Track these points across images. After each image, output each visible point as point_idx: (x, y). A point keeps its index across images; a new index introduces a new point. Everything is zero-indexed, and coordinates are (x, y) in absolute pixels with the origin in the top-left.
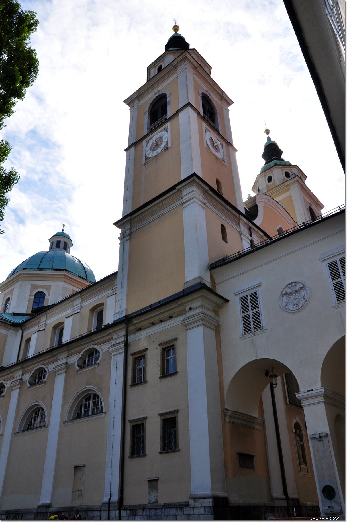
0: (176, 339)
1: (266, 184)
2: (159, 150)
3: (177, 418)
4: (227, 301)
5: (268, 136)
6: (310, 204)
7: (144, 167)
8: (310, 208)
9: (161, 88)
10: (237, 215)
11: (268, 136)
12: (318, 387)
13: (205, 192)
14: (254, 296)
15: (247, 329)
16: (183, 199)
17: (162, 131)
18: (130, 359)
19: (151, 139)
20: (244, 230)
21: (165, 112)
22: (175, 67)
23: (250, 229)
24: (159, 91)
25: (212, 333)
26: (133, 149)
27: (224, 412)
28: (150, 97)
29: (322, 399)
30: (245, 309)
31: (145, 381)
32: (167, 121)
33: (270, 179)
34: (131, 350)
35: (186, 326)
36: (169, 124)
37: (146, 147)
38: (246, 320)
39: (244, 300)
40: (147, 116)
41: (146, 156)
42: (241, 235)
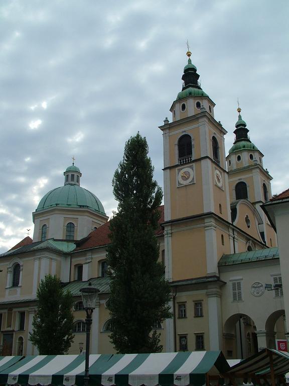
0: (203, 300)
3: (205, 337)
4: (226, 283)
6: (264, 181)
8: (264, 185)
9: (187, 129)
10: (228, 225)
12: (264, 330)
13: (216, 219)
14: (239, 284)
15: (235, 299)
16: (206, 224)
17: (189, 167)
18: (177, 305)
19: (181, 169)
20: (231, 231)
21: (190, 153)
22: (198, 118)
23: (233, 230)
24: (185, 131)
25: (219, 299)
26: (168, 170)
27: (223, 333)
28: (178, 133)
29: (265, 335)
30: (234, 289)
31: (185, 317)
32: (191, 162)
33: (239, 158)
34: (177, 301)
35: (208, 295)
36: (194, 164)
38: (234, 295)
39: (234, 285)
42: (229, 236)
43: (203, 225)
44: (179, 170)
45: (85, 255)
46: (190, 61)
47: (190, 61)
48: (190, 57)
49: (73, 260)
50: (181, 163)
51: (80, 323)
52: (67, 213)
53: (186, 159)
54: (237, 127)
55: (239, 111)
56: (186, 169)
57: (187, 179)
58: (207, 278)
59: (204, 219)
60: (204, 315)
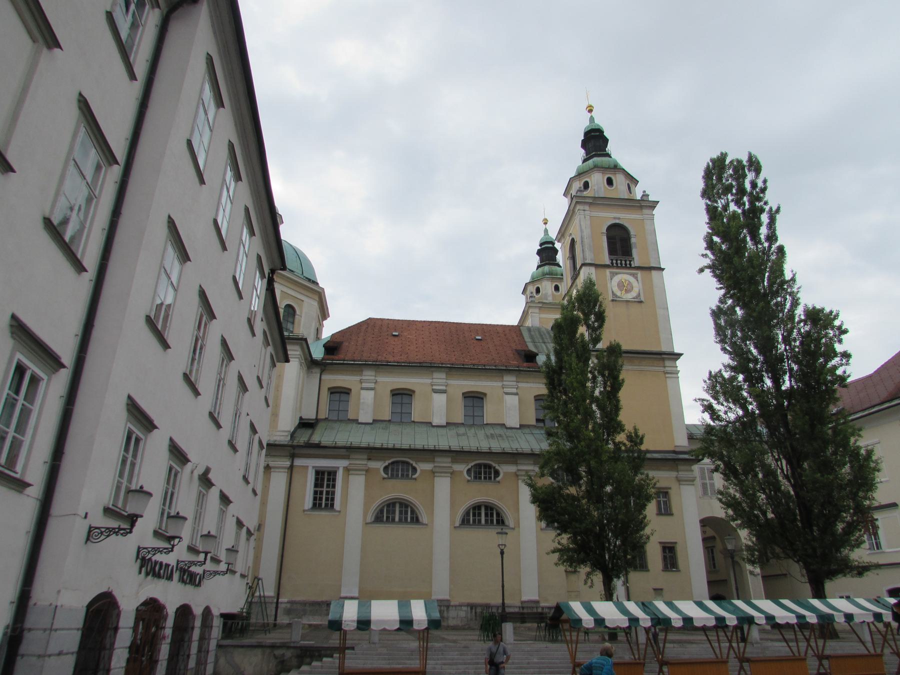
1: (552, 291)
2: (630, 296)
3: (679, 550)
5: (546, 228)
7: (611, 303)
11: (546, 228)
17: (631, 275)
19: (617, 274)
24: (619, 219)
28: (611, 216)
36: (639, 274)
37: (611, 279)
40: (605, 239)
41: (613, 292)
43: (662, 369)
44: (613, 275)
45: (360, 373)
46: (592, 119)
47: (592, 119)
48: (593, 114)
49: (323, 377)
50: (612, 263)
51: (394, 504)
52: (289, 285)
53: (621, 261)
54: (541, 245)
55: (545, 223)
56: (624, 276)
57: (627, 291)
58: (674, 452)
59: (663, 359)
60: (674, 510)
